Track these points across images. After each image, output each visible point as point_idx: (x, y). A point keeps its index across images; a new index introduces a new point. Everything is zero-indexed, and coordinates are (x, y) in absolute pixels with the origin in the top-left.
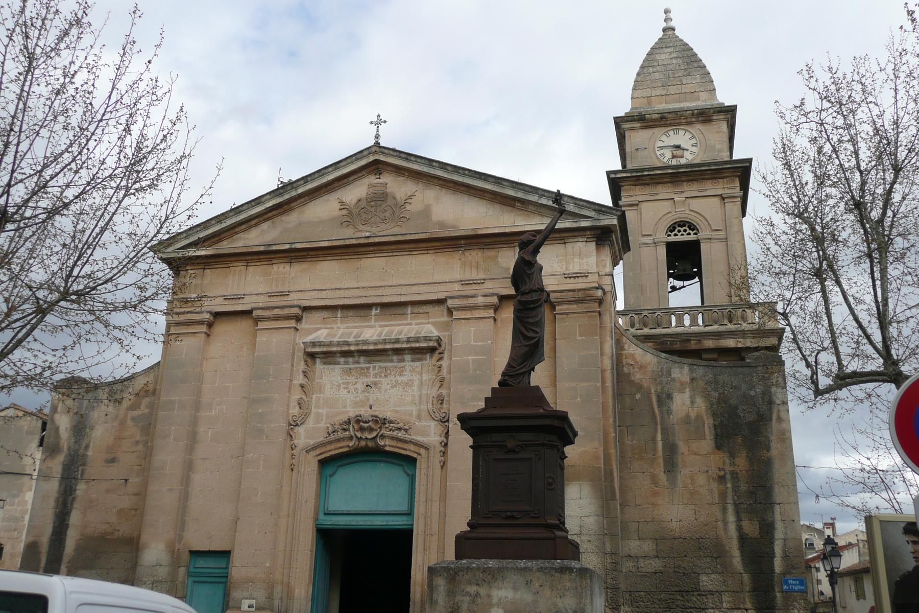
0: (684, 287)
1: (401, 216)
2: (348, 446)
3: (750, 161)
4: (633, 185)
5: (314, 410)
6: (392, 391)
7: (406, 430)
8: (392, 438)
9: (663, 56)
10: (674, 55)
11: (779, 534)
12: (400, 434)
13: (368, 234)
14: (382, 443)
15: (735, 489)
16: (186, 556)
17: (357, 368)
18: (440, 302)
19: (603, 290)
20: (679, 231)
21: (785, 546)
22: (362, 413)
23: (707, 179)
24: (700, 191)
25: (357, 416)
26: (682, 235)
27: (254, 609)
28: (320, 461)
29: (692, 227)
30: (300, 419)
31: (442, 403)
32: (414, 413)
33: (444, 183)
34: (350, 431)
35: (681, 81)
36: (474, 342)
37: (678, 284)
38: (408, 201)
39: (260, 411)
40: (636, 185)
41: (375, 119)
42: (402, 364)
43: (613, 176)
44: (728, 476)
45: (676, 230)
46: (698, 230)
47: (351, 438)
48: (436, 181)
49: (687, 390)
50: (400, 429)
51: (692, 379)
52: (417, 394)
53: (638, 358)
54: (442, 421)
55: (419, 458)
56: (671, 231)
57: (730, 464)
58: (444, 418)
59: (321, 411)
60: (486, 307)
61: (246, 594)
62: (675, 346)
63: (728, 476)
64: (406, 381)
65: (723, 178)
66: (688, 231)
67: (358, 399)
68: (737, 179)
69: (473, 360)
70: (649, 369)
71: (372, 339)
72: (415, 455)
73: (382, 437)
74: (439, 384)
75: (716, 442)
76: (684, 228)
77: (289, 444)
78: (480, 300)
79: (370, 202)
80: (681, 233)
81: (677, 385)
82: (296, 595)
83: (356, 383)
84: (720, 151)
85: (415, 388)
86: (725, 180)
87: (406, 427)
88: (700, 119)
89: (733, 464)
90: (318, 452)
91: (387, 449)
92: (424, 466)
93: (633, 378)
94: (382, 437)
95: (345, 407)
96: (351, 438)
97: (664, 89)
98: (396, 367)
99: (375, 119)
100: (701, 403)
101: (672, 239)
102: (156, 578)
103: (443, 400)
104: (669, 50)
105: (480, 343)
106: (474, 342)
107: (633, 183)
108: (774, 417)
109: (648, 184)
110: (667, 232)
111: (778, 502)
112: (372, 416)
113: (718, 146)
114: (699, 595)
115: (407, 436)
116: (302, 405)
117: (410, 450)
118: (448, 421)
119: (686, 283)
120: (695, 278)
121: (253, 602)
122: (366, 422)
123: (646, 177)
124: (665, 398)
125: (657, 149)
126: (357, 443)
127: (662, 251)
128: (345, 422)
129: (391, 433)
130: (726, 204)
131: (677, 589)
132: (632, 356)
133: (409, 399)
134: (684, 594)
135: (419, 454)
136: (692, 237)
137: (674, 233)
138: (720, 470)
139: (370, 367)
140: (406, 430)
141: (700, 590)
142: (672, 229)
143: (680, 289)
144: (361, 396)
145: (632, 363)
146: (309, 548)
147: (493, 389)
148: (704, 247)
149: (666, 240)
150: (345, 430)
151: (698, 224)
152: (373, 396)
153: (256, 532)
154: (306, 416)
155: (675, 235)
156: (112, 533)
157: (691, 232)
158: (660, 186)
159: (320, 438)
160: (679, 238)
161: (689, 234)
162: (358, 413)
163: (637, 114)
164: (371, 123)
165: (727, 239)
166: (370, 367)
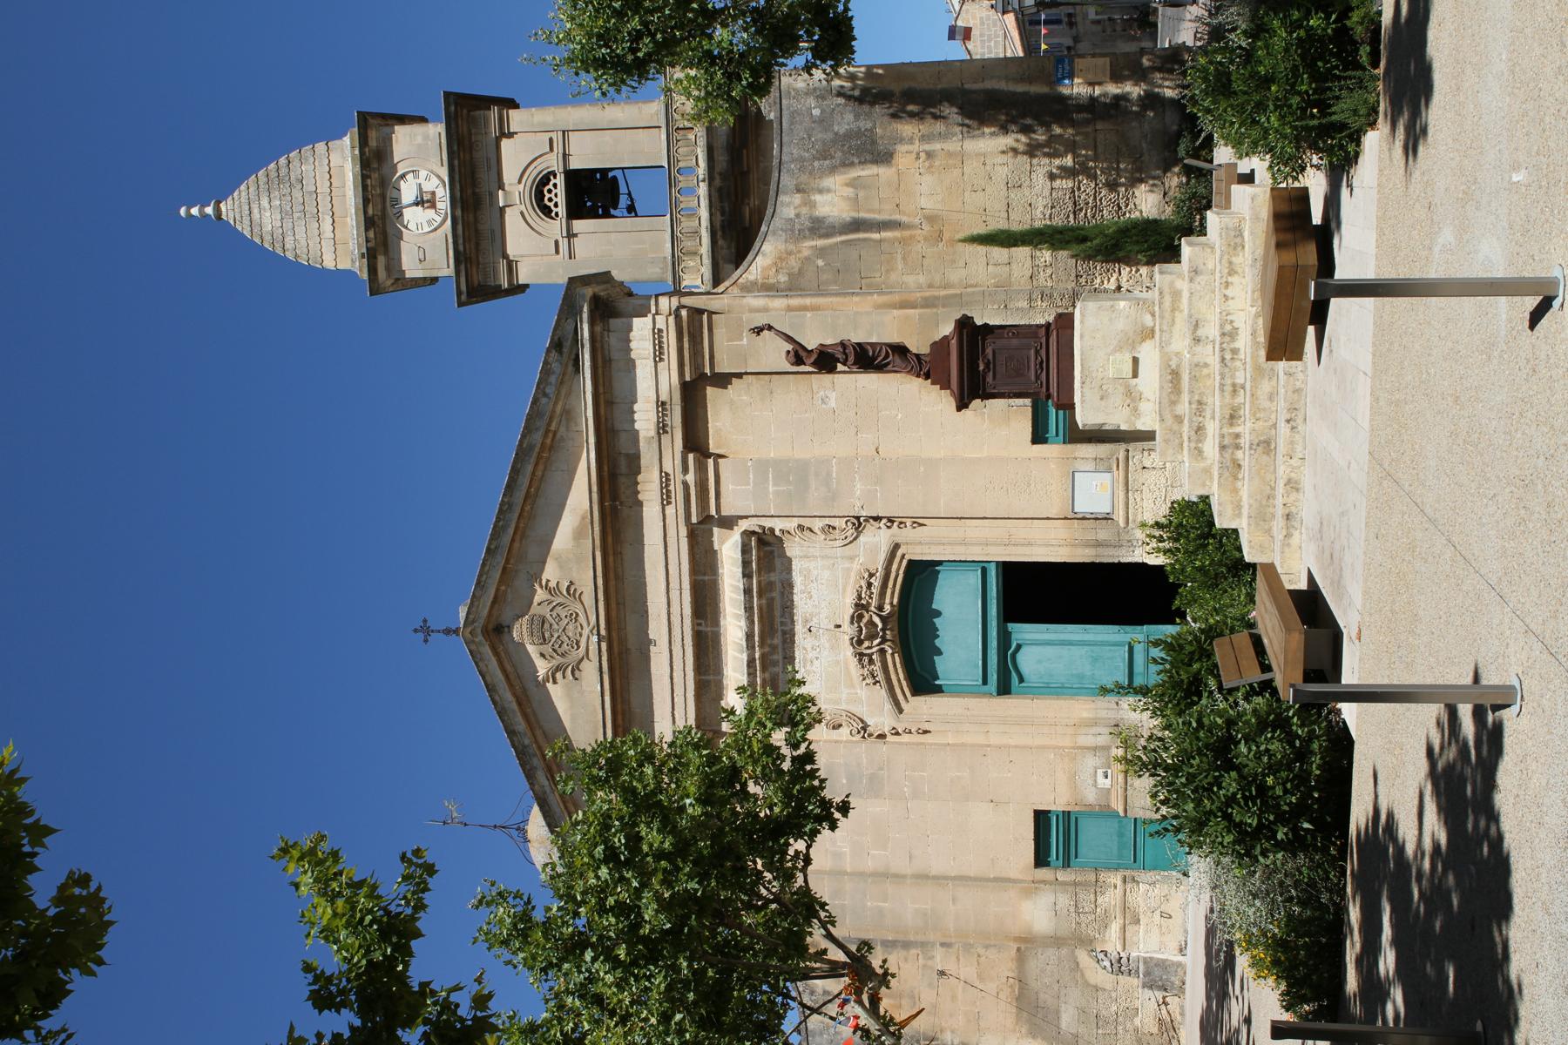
0: (629, 194)
1: (565, 593)
2: (893, 654)
3: (447, 95)
4: (478, 268)
5: (844, 707)
6: (815, 597)
7: (871, 575)
8: (882, 594)
9: (266, 221)
10: (265, 202)
11: (1002, 86)
12: (876, 582)
13: (595, 638)
14: (887, 608)
15: (942, 137)
16: (1043, 873)
17: (784, 649)
18: (693, 535)
19: (678, 309)
20: (550, 200)
22: (847, 638)
23: (472, 158)
24: (489, 168)
25: (852, 644)
26: (556, 195)
27: (1110, 771)
28: (914, 694)
29: (545, 180)
30: (855, 725)
31: (834, 528)
32: (847, 565)
33: (519, 533)
34: (873, 654)
35: (310, 193)
36: (749, 484)
37: (624, 201)
38: (544, 584)
39: (844, 781)
40: (478, 264)
41: (421, 635)
42: (779, 585)
43: (464, 297)
44: (927, 147)
45: (548, 204)
46: (549, 173)
47: (882, 652)
48: (516, 545)
49: (813, 198)
50: (870, 585)
51: (798, 191)
52: (820, 562)
53: (768, 261)
54: (859, 526)
55: (907, 557)
57: (911, 143)
58: (854, 524)
59: (844, 696)
60: (701, 469)
61: (1090, 782)
62: (727, 209)
63: (927, 147)
64: (802, 578)
65: (470, 134)
66: (550, 186)
67: (827, 645)
68: (472, 113)
69: (774, 485)
70: (782, 247)
71: (744, 627)
72: (905, 563)
73: (880, 608)
74: (807, 533)
75: (882, 162)
76: (546, 192)
77: (890, 738)
78: (690, 478)
79: (545, 640)
80: (554, 198)
81: (804, 211)
82: (1091, 716)
83: (805, 649)
84: (426, 137)
85: (812, 565)
86: (473, 131)
87: (866, 576)
88: (375, 165)
89: (911, 141)
90: (900, 697)
91: (895, 601)
92: (918, 549)
93: (796, 270)
94: (880, 608)
95: (838, 662)
96: (882, 652)
97: (324, 219)
98: (783, 593)
99: (421, 635)
100: (828, 182)
101: (562, 210)
102: (1072, 909)
103: (829, 526)
104: (255, 211)
105: (751, 476)
106: (749, 484)
107: (474, 269)
109: (477, 244)
110: (552, 218)
111: (960, 85)
112: (852, 623)
113: (419, 139)
114: (1079, 189)
115: (878, 574)
116: (836, 723)
117: (899, 570)
118: (858, 518)
119: (623, 189)
120: (615, 178)
121: (1100, 772)
122: (861, 630)
123: (467, 247)
124: (819, 227)
125: (420, 231)
126: (889, 643)
127: (579, 225)
128: (860, 660)
129: (874, 596)
130: (512, 131)
131: (1071, 216)
132: (764, 269)
133: (826, 574)
134: (1078, 207)
135: (903, 556)
136: (560, 180)
137: (553, 208)
138: (918, 158)
139: (782, 630)
140: (871, 575)
141: (1073, 188)
142: (547, 211)
143: (632, 200)
144: (824, 640)
145: (774, 270)
146: (1029, 701)
147: (933, 383)
148: (575, 164)
149: (564, 220)
150: (871, 662)
151: (541, 172)
152: (823, 621)
153: (1009, 775)
154: (852, 716)
155: (556, 205)
156: (1011, 986)
157: (551, 183)
158: (481, 227)
159: (881, 692)
160: (561, 199)
161: (555, 186)
162: (848, 642)
163: (365, 260)
164: (426, 641)
165: (564, 132)
166: (782, 630)
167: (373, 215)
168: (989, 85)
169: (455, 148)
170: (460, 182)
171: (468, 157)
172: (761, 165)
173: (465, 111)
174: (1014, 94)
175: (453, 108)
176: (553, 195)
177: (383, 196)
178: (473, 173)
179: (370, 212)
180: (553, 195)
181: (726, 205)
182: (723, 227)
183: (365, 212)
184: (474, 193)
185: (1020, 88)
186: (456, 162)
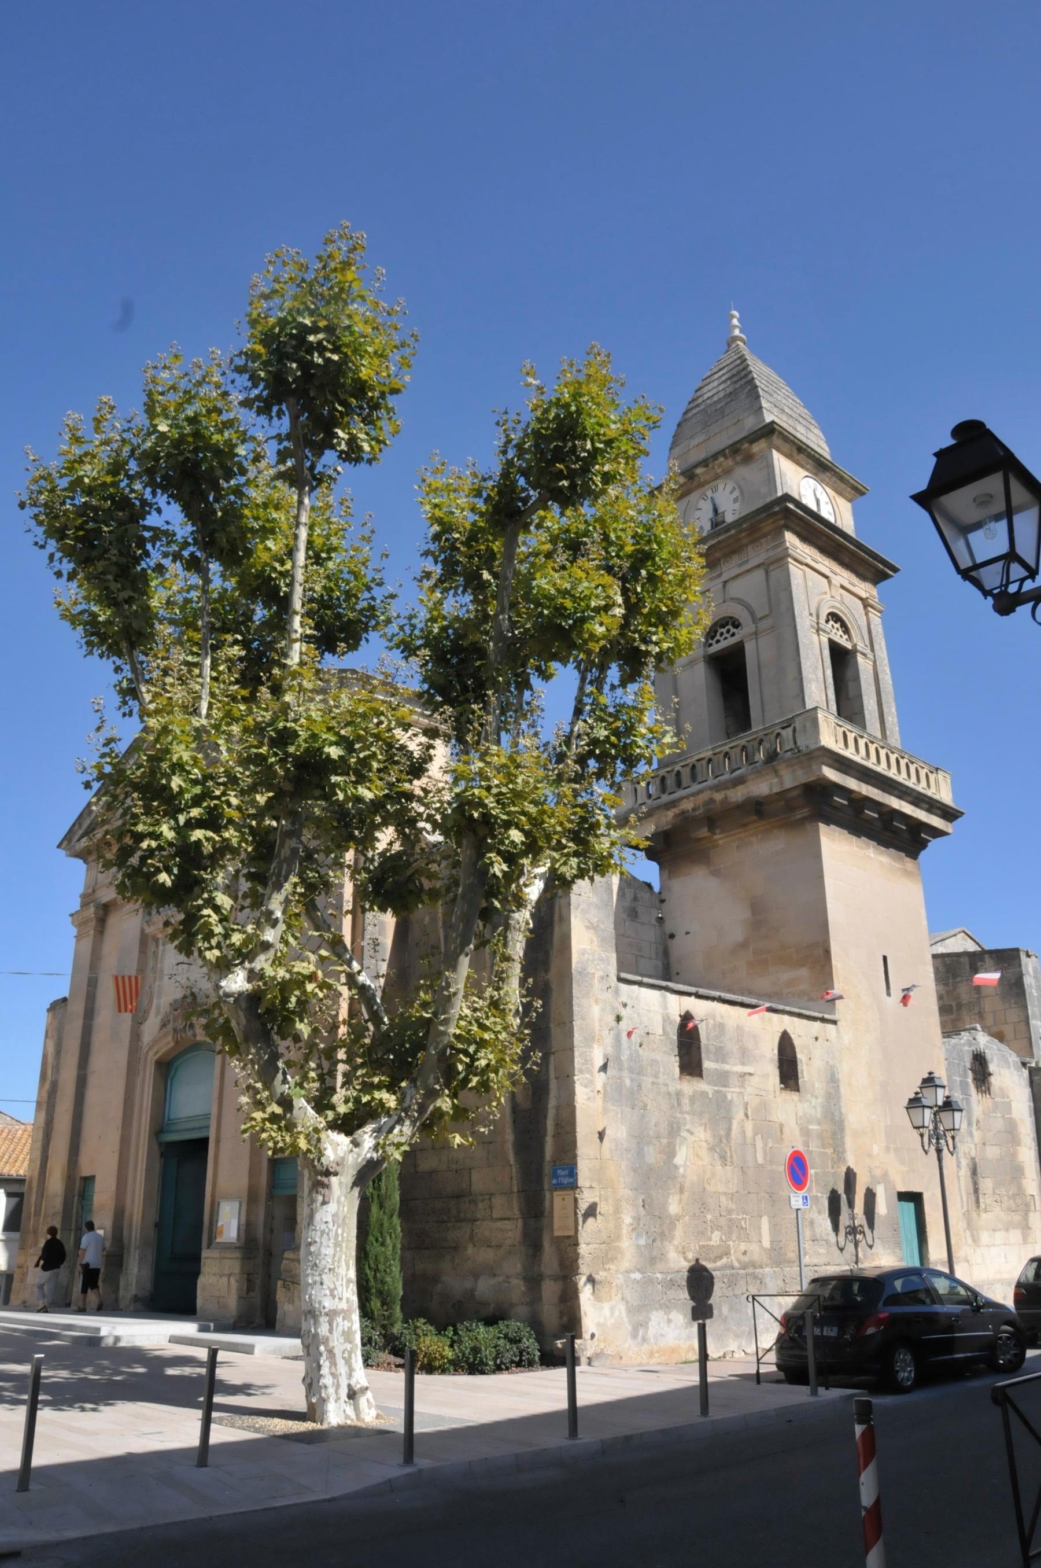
11: (552, 1103)
20: (722, 634)
21: (557, 1115)
23: (747, 546)
26: (726, 638)
56: (712, 638)
65: (765, 536)
66: (733, 630)
88: (738, 458)
108: (556, 918)
155: (718, 641)
160: (723, 644)
167: (697, 475)
168: (553, 1085)
169: (744, 526)
170: (719, 542)
171: (745, 541)
172: (754, 838)
173: (782, 522)
174: (545, 1117)
175: (777, 509)
176: (725, 635)
177: (717, 477)
178: (734, 552)
179: (699, 471)
180: (725, 635)
181: (701, 811)
182: (683, 812)
183: (696, 466)
184: (719, 560)
185: (550, 1124)
186: (733, 532)
